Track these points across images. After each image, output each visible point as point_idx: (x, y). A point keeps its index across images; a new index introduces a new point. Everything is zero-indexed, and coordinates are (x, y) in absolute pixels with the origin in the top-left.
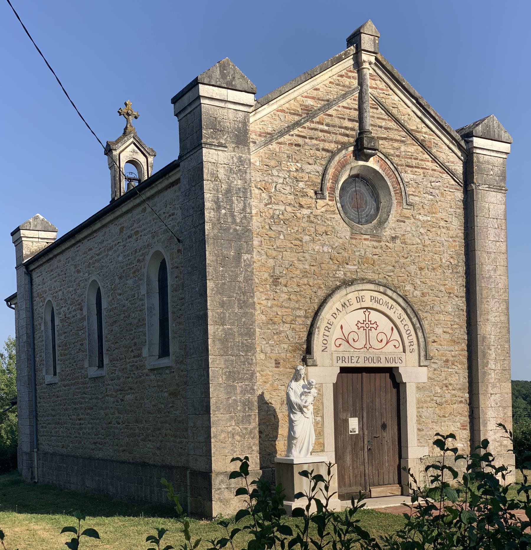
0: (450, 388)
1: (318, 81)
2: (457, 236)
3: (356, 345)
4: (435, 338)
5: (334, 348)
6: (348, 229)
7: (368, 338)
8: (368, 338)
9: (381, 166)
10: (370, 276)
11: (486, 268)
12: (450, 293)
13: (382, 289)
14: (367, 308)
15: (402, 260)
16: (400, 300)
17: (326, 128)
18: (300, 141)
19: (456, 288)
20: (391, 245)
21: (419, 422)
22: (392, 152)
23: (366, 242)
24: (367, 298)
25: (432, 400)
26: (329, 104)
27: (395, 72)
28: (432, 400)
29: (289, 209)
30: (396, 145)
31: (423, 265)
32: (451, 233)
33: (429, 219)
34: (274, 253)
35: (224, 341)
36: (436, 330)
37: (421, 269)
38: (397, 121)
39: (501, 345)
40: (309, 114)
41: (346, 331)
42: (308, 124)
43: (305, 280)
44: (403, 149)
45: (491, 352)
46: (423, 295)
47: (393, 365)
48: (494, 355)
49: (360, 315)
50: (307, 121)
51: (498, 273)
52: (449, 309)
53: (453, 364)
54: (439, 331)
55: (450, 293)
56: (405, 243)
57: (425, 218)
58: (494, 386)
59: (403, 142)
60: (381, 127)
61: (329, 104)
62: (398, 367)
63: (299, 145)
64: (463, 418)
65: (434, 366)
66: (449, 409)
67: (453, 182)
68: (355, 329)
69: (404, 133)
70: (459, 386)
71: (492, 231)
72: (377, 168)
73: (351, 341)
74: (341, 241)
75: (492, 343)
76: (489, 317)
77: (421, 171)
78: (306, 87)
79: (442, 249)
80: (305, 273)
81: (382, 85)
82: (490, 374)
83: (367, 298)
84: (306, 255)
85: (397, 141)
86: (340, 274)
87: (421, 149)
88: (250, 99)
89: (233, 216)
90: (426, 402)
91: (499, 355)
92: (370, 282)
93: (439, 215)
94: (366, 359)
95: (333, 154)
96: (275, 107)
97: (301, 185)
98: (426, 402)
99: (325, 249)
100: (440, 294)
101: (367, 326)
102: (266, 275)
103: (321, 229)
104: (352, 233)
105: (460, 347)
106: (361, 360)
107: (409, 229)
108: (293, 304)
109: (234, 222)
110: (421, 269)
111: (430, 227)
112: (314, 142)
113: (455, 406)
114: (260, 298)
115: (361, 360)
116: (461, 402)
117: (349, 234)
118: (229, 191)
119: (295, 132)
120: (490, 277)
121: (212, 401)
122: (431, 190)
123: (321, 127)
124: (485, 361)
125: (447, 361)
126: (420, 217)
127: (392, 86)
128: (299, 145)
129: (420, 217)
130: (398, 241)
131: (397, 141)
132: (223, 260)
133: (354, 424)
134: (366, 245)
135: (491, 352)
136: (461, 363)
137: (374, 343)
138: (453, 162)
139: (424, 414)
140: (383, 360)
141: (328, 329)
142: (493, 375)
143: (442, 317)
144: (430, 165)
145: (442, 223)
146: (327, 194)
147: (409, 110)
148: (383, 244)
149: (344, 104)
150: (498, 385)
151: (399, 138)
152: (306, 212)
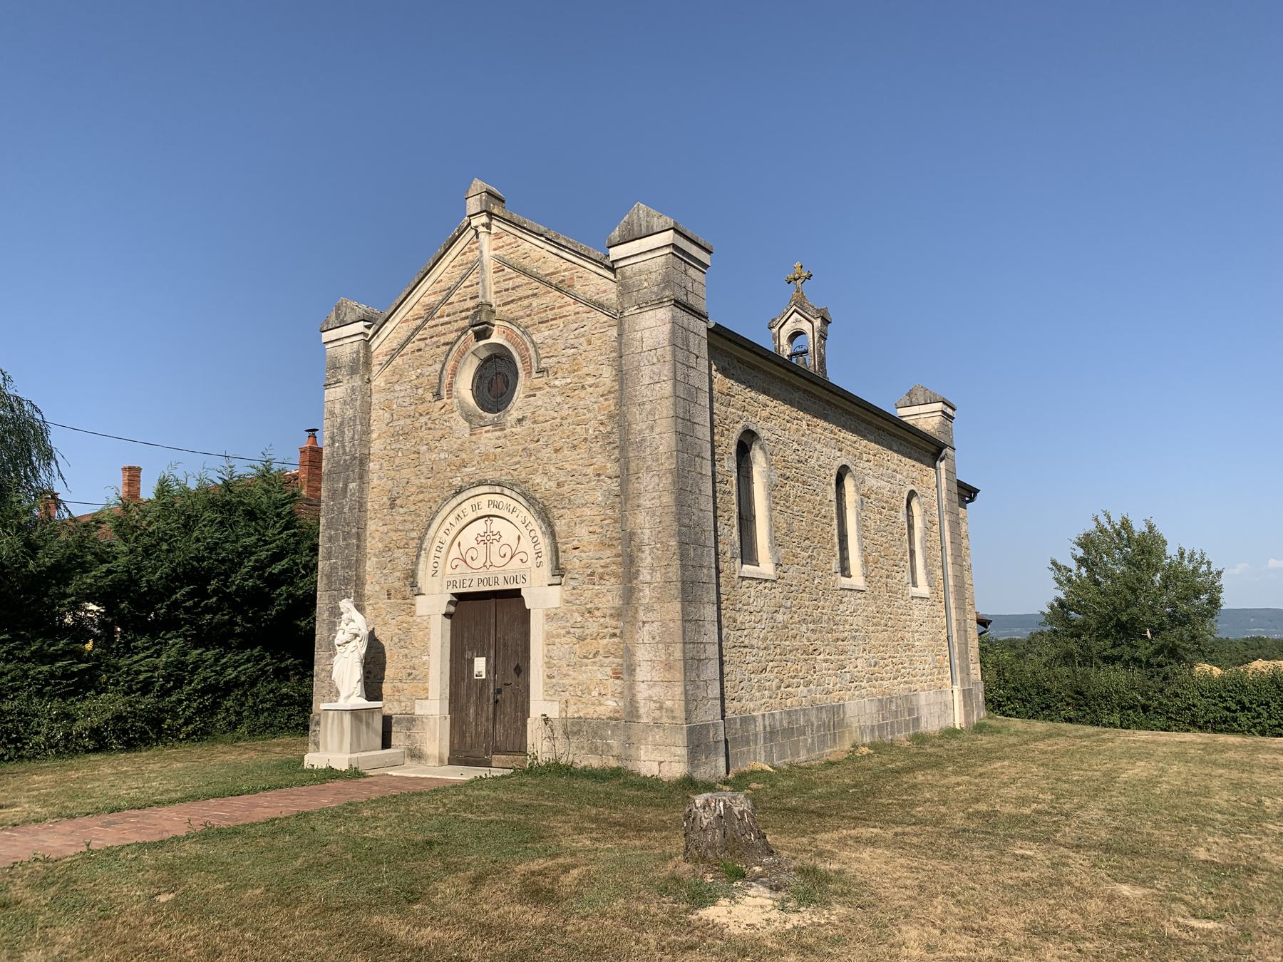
0: (597, 613)
1: (439, 272)
2: (610, 392)
3: (474, 564)
4: (575, 543)
5: (449, 570)
6: (467, 425)
7: (488, 555)
8: (488, 555)
9: (507, 339)
10: (490, 475)
11: (636, 428)
12: (599, 475)
13: (498, 489)
14: (489, 516)
15: (533, 446)
16: (521, 499)
17: (446, 319)
18: (422, 344)
19: (609, 465)
20: (518, 430)
21: (549, 665)
22: (521, 313)
23: (488, 435)
24: (484, 505)
25: (568, 633)
26: (450, 291)
27: (516, 217)
28: (568, 633)
29: (409, 421)
30: (526, 302)
31: (557, 445)
32: (600, 390)
33: (569, 380)
34: (392, 473)
35: (329, 576)
36: (577, 530)
37: (557, 451)
38: (524, 272)
39: (662, 543)
40: (431, 311)
41: (464, 549)
42: (430, 323)
43: (421, 496)
44: (534, 304)
45: (643, 556)
46: (559, 485)
47: (515, 586)
48: (649, 560)
49: (480, 526)
50: (427, 320)
51: (657, 430)
52: (599, 496)
53: (601, 578)
54: (582, 531)
55: (599, 475)
56: (535, 422)
57: (564, 381)
58: (649, 609)
59: (535, 295)
60: (507, 290)
61: (450, 291)
62: (519, 590)
63: (419, 350)
64: (617, 660)
65: (573, 583)
66: (592, 645)
67: (606, 318)
68: (474, 544)
69: (537, 284)
70: (609, 612)
71: (646, 371)
72: (501, 341)
73: (469, 560)
74: (459, 441)
75: (646, 541)
76: (641, 501)
77: (560, 322)
78: (426, 285)
79: (588, 415)
80: (421, 490)
81: (511, 239)
82: (641, 591)
83: (484, 505)
84: (423, 468)
85: (527, 297)
86: (457, 482)
87: (557, 293)
88: (359, 327)
89: (344, 447)
90: (558, 636)
91: (658, 558)
92: (481, 483)
93: (585, 370)
94: (481, 581)
95: (452, 344)
96: (397, 320)
97: (420, 391)
98: (558, 636)
99: (442, 456)
100: (584, 479)
101: (488, 539)
102: (385, 499)
103: (438, 434)
104: (471, 429)
105: (614, 552)
106: (475, 583)
107: (540, 403)
108: (408, 526)
109: (344, 453)
110: (557, 451)
111: (566, 392)
112: (435, 339)
113: (605, 641)
114: (373, 527)
115: (475, 583)
116: (614, 635)
117: (468, 431)
118: (342, 423)
119: (417, 337)
120: (643, 440)
121: (317, 638)
122: (572, 342)
123: (442, 320)
124: (633, 570)
125: (592, 574)
126: (557, 383)
127: (519, 234)
128: (419, 350)
129: (557, 383)
130: (527, 423)
131: (527, 297)
132: (333, 493)
133: (480, 665)
134: (488, 438)
135: (643, 556)
136: (614, 574)
137: (497, 560)
138: (605, 291)
139: (555, 653)
140: (501, 580)
141: (439, 549)
142: (647, 592)
143: (587, 512)
144: (572, 308)
145: (590, 380)
146: (444, 392)
147: (544, 253)
148: (508, 431)
149: (467, 283)
150: (656, 606)
151: (530, 292)
152: (423, 419)
